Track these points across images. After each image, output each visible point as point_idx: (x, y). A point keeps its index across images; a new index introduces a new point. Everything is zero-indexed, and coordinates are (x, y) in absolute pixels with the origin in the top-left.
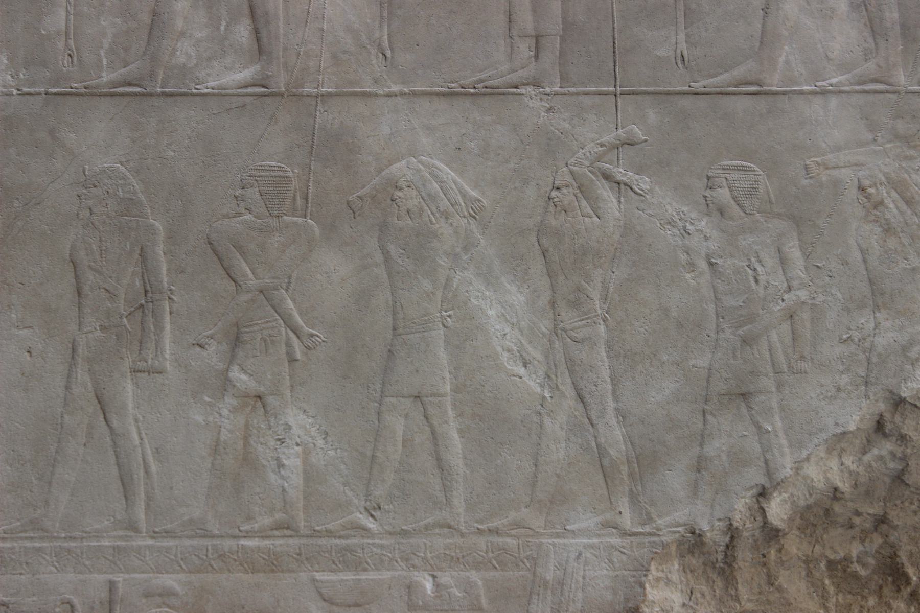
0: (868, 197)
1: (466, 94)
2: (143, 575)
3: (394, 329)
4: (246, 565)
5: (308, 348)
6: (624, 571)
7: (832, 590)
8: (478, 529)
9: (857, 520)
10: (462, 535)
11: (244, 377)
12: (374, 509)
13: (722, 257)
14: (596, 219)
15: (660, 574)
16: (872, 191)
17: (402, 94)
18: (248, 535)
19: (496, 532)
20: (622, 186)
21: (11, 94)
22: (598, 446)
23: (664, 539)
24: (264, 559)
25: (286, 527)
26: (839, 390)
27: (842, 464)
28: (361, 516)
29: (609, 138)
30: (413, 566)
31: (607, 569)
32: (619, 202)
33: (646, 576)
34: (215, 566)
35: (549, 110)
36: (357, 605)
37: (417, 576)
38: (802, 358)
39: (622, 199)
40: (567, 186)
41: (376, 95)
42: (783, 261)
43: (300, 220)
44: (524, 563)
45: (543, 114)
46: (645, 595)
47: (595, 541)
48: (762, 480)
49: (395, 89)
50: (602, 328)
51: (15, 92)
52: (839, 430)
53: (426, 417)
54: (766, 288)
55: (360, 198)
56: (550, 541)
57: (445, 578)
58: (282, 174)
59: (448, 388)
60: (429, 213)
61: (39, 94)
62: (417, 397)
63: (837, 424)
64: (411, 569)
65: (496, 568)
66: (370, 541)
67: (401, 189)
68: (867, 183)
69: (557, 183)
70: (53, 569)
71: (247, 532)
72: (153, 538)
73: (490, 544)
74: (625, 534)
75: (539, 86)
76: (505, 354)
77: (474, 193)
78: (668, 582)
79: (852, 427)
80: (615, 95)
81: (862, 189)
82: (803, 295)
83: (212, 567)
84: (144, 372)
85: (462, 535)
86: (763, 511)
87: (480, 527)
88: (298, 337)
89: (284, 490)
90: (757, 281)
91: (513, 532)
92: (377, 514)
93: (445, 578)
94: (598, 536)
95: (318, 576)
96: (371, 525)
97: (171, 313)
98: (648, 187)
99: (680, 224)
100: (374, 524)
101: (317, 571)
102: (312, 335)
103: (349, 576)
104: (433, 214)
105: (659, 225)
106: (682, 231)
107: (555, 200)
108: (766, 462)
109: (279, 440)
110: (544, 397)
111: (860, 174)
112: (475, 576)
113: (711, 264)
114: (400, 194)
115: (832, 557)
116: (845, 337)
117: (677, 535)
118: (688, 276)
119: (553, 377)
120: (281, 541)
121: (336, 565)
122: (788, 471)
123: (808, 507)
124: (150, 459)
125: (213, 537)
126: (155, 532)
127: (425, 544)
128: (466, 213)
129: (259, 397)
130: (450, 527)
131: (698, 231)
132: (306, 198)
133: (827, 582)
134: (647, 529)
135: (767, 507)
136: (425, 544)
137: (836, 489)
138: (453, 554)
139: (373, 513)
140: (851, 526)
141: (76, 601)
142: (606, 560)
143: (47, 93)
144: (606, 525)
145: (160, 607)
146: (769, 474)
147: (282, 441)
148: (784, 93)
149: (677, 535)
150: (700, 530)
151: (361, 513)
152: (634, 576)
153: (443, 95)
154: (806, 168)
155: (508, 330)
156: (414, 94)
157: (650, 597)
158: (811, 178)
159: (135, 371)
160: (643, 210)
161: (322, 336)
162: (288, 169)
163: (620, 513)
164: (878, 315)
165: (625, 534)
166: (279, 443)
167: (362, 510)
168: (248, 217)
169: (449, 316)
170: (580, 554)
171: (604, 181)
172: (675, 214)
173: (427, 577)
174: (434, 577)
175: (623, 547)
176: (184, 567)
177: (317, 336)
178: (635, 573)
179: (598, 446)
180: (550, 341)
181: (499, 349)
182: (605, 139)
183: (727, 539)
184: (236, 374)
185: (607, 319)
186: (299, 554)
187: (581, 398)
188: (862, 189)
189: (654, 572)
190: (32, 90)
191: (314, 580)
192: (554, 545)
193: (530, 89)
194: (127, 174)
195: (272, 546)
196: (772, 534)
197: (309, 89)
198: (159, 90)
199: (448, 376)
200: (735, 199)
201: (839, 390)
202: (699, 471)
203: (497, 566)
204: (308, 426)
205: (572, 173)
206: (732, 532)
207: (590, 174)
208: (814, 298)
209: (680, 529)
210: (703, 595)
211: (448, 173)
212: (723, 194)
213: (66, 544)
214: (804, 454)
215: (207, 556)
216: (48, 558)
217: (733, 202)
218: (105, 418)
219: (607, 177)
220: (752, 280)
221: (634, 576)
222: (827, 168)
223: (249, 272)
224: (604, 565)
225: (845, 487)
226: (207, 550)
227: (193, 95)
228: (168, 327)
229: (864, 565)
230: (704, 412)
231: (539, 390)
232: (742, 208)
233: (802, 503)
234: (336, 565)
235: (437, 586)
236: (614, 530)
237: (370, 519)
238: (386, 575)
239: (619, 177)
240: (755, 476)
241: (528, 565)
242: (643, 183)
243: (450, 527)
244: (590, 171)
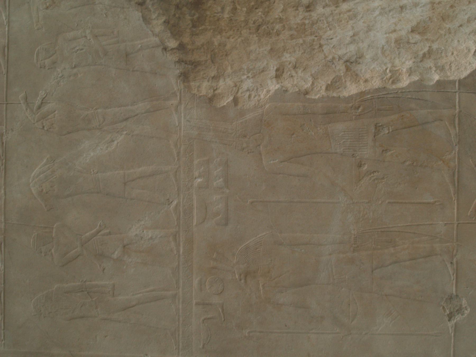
0: (50, 6)
1: (5, 163)
2: (194, 292)
3: (98, 193)
4: (190, 252)
5: (105, 227)
6: (195, 104)
7: (203, 27)
8: (177, 160)
9: (177, 16)
10: (180, 167)
11: (116, 253)
12: (169, 201)
13: (72, 63)
14: (56, 112)
15: (196, 90)
16: (48, 4)
17: (5, 189)
18: (178, 251)
19: (178, 153)
20: (43, 102)
21: (4, 343)
22: (145, 113)
23: (182, 87)
24: (188, 245)
25: (175, 236)
26: (125, 19)
27: (155, 19)
28: (172, 207)
29: (24, 107)
30: (191, 186)
31: (194, 110)
32: (49, 103)
33: (196, 95)
34: (190, 264)
35: (12, 130)
36: (206, 209)
37: (195, 185)
38: (113, 32)
39: (48, 102)
40: (43, 124)
41: (5, 199)
42: (75, 39)
43: (54, 230)
44: (190, 143)
45: (14, 133)
46: (204, 96)
47: (182, 115)
48: (160, 49)
49: (3, 192)
50: (99, 110)
51: (3, 342)
52: (141, 19)
53: (133, 180)
54: (85, 46)
55: (46, 206)
56: (182, 132)
57: (196, 174)
58: (36, 237)
59: (121, 172)
60: (52, 179)
61: (4, 333)
62: (125, 184)
63: (139, 20)
64: (192, 187)
65: (193, 154)
66: (181, 203)
67: (42, 190)
68: (45, 6)
69: (41, 127)
70: (190, 327)
71: (177, 252)
72: (179, 288)
73: (183, 156)
74: (180, 103)
75: (3, 134)
76: (109, 149)
77: (45, 161)
78: (199, 87)
79: (140, 14)
80: (7, 104)
81: (47, 8)
82: (88, 31)
83: (191, 265)
84: (114, 292)
85: (180, 167)
86: (172, 49)
87: (176, 160)
88: (101, 231)
89: (161, 237)
90: (82, 49)
91: (179, 147)
92: (171, 200)
93: (196, 174)
94: (181, 113)
95: (195, 224)
96: (175, 203)
97: (91, 281)
98: (44, 92)
99: (59, 79)
100: (174, 202)
101: (193, 224)
102: (100, 226)
103: (195, 211)
104: (53, 177)
105: (59, 87)
106: (62, 78)
107: (48, 128)
108: (153, 47)
109: (141, 239)
110: (126, 134)
111: (41, 9)
112: (196, 162)
113: (75, 67)
114: (44, 190)
115: (191, 26)
116: (105, 16)
117: (181, 82)
118: (79, 76)
119: (118, 130)
120: (181, 238)
121: (190, 217)
122: (157, 39)
123: (171, 33)
124: (148, 289)
125: (179, 265)
126: (177, 287)
127: (183, 181)
128: (53, 164)
129: (124, 247)
130: (176, 172)
131: (62, 72)
132: (46, 228)
133: (200, 28)
134: (178, 94)
135: (171, 47)
136: (183, 181)
137: (164, 22)
138: (187, 170)
139: (170, 202)
140: (179, 18)
141: (203, 318)
142: (190, 110)
143: (4, 329)
144: (176, 110)
145: (206, 286)
146: (158, 46)
147: (142, 238)
148: (8, 37)
149: (181, 82)
150: (179, 73)
151: (170, 207)
152: (197, 100)
153: (5, 172)
154: (38, 29)
155: (99, 148)
156: (5, 183)
157: (205, 94)
158: (42, 28)
159: (113, 295)
160: (53, 93)
161: (101, 221)
162: (34, 234)
163: (172, 104)
164: (97, 3)
165: (180, 103)
166: (142, 239)
167: (169, 206)
168: (53, 251)
169: (93, 171)
170: (188, 121)
171: (41, 109)
172: (55, 81)
173: (196, 181)
174: (196, 178)
175: (185, 104)
176: (190, 276)
177: (100, 223)
178: (195, 99)
179: (145, 113)
180: (104, 131)
181: (107, 151)
182: (25, 109)
183: (183, 63)
184: (115, 256)
185: (96, 108)
186: (186, 231)
187: (126, 119)
188: (47, 8)
189: (195, 91)
190: (3, 335)
191: (196, 225)
192: (184, 131)
193: (4, 138)
194: (35, 298)
195: (183, 242)
196: (181, 47)
197: (3, 227)
198: (3, 285)
199: (117, 172)
200: (49, 57)
201: (125, 19)
202: (156, 73)
203: (192, 153)
204: (136, 227)
205: (37, 122)
206: (180, 61)
207: (38, 114)
208: (89, 27)
209: (179, 81)
210: (204, 74)
211: (36, 171)
212: (47, 62)
213: (181, 322)
214: (150, 32)
215: (186, 267)
216: (186, 329)
217: (51, 58)
218: (132, 307)
219: (39, 107)
220: (82, 51)
221: (197, 100)
222: (39, 21)
223: (74, 251)
224: (192, 111)
225: (163, 19)
226: (184, 267)
227: (4, 272)
228: (96, 282)
229: (194, 15)
230: (133, 71)
231: (123, 136)
232: (53, 54)
233: (169, 34)
234: (190, 217)
235: (199, 177)
236: (179, 107)
237: (173, 203)
238: (195, 197)
239: (40, 103)
240: (159, 52)
241: (192, 141)
242: (42, 93)
243: (176, 172)
244: (37, 114)
